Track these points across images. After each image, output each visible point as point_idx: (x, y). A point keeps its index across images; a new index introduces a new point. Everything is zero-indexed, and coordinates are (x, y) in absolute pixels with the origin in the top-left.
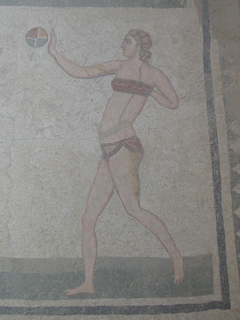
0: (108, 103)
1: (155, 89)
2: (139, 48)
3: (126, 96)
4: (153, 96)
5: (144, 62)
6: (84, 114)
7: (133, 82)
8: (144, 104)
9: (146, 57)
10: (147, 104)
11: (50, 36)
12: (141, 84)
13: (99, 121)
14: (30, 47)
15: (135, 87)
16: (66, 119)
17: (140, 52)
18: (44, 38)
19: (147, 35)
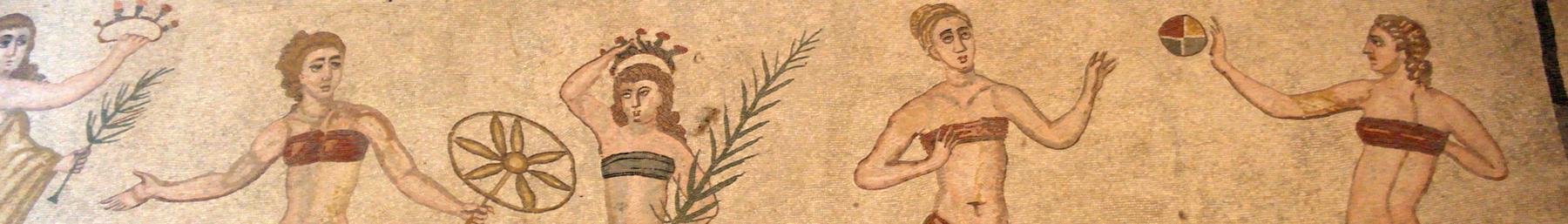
0: (1356, 169)
1: (1452, 138)
2: (1403, 55)
3: (1392, 155)
4: (1449, 155)
5: (1419, 82)
6: (1309, 194)
7: (1404, 126)
8: (1432, 170)
9: (1422, 74)
10: (1439, 171)
11: (1212, 32)
12: (1419, 129)
13: (1343, 207)
14: (1172, 56)
15: (1408, 136)
16: (1272, 204)
17: (1407, 63)
18: (1198, 36)
19: (1416, 26)
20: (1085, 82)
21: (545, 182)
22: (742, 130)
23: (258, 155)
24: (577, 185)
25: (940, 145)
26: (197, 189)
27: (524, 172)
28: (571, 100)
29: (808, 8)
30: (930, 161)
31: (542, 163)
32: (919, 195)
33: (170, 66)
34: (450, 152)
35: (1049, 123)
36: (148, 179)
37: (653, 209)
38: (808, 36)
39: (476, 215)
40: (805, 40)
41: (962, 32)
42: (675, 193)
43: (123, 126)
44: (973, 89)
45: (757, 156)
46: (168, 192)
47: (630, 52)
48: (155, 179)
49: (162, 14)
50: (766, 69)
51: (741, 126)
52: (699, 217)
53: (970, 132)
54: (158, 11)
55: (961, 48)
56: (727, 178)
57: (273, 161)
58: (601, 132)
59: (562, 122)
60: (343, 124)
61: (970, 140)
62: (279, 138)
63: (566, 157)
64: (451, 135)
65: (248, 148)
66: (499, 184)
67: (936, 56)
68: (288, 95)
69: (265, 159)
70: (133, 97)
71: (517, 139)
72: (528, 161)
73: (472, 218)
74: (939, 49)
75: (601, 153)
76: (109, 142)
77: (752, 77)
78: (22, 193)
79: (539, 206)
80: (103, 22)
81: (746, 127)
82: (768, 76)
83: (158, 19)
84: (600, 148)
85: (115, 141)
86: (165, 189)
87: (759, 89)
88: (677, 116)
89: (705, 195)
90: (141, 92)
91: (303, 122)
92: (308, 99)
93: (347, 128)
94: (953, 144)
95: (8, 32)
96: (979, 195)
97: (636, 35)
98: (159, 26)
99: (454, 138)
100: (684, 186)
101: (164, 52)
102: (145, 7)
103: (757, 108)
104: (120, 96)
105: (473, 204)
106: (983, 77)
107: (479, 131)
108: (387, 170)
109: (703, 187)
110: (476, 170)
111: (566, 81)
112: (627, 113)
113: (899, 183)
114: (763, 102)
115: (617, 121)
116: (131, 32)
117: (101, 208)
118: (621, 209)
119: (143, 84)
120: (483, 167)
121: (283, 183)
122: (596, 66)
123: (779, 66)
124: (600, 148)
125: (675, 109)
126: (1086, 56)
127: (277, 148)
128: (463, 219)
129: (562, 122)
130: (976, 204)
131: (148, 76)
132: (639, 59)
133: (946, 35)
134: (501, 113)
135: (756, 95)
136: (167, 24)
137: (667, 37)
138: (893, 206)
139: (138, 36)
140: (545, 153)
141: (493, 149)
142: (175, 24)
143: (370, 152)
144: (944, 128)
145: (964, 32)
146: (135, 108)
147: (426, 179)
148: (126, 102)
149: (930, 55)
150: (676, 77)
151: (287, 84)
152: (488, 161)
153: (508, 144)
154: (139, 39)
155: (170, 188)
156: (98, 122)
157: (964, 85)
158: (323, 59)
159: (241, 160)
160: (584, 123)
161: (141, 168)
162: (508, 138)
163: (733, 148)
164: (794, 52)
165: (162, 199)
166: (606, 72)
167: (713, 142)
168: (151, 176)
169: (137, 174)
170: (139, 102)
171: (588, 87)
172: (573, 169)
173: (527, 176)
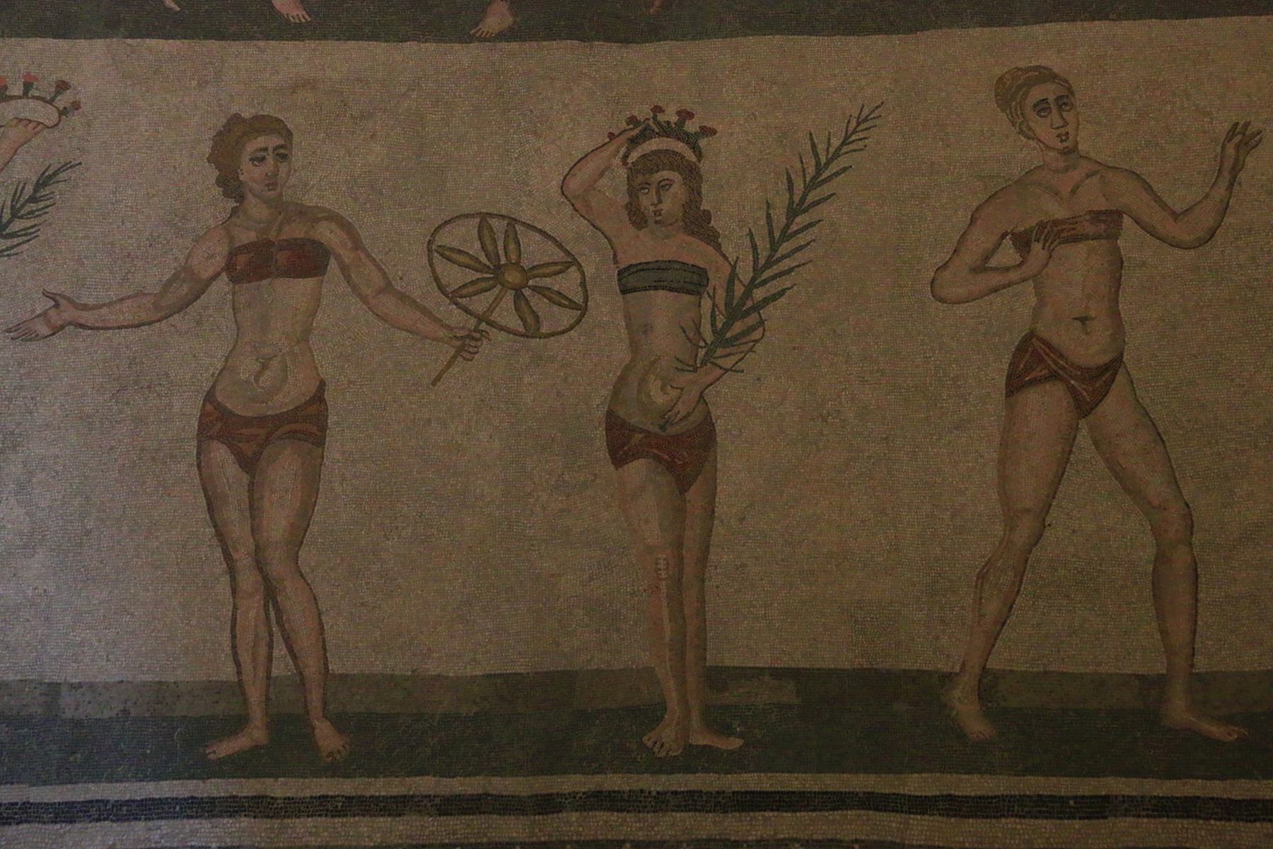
20: (1222, 162)
21: (550, 299)
22: (789, 231)
23: (196, 272)
24: (589, 304)
25: (1036, 247)
26: (126, 313)
27: (524, 288)
28: (574, 197)
29: (865, 75)
30: (1024, 267)
31: (545, 276)
32: (1012, 310)
33: (74, 159)
34: (431, 265)
35: (1175, 215)
36: (62, 301)
37: (684, 332)
38: (866, 111)
39: (467, 341)
40: (863, 117)
41: (1060, 102)
42: (710, 310)
43: (25, 235)
44: (1076, 175)
45: (809, 265)
46: (88, 317)
47: (646, 135)
49: (58, 93)
50: (816, 155)
51: (787, 226)
52: (740, 341)
53: (1074, 229)
54: (53, 89)
55: (1061, 123)
56: (773, 291)
57: (216, 276)
58: (614, 236)
59: (565, 224)
60: (297, 231)
61: (1075, 239)
62: (221, 250)
63: (573, 268)
64: (430, 242)
65: (183, 261)
66: (494, 302)
67: (1031, 134)
68: (227, 194)
69: (205, 275)
70: (33, 199)
71: (512, 246)
72: (528, 273)
73: (464, 345)
74: (1032, 124)
75: (616, 262)
76: (8, 255)
77: (798, 165)
79: (544, 330)
81: (794, 228)
82: (818, 163)
83: (53, 100)
84: (615, 256)
86: (84, 314)
87: (808, 180)
88: (707, 216)
89: (747, 313)
91: (247, 229)
92: (250, 196)
93: (302, 235)
94: (1056, 243)
96: (1087, 308)
97: (652, 115)
98: (57, 109)
99: (434, 247)
100: (721, 302)
101: (66, 141)
103: (806, 205)
104: (15, 199)
105: (463, 328)
106: (1089, 159)
107: (463, 236)
108: (355, 288)
109: (745, 304)
110: (465, 286)
111: (568, 174)
112: (646, 212)
113: (987, 295)
114: (812, 197)
115: (634, 223)
116: (22, 116)
118: (645, 332)
119: (43, 182)
120: (472, 282)
121: (229, 305)
122: (606, 153)
123: (832, 150)
124: (615, 256)
125: (705, 206)
126: (1223, 128)
127: (219, 261)
128: (453, 346)
129: (565, 224)
130: (1083, 320)
131: (50, 172)
132: (654, 145)
133: (1038, 108)
134: (491, 215)
135: (805, 188)
136: (68, 105)
137: (690, 115)
138: (981, 323)
139: (30, 121)
140: (548, 264)
141: (483, 259)
142: (76, 106)
143: (333, 264)
144: (1042, 225)
145: (1064, 101)
146: (37, 213)
147: (403, 297)
149: (1021, 132)
150: (704, 166)
151: (221, 182)
152: (479, 275)
153: (501, 252)
154: (31, 125)
155: (90, 313)
157: (1066, 169)
158: (265, 149)
159: (175, 277)
160: (594, 226)
161: (51, 288)
162: (500, 244)
163: (778, 255)
164: (849, 134)
166: (617, 161)
167: (754, 247)
168: (64, 297)
169: (46, 294)
170: (41, 205)
171: (595, 181)
172: (583, 284)
173: (527, 292)
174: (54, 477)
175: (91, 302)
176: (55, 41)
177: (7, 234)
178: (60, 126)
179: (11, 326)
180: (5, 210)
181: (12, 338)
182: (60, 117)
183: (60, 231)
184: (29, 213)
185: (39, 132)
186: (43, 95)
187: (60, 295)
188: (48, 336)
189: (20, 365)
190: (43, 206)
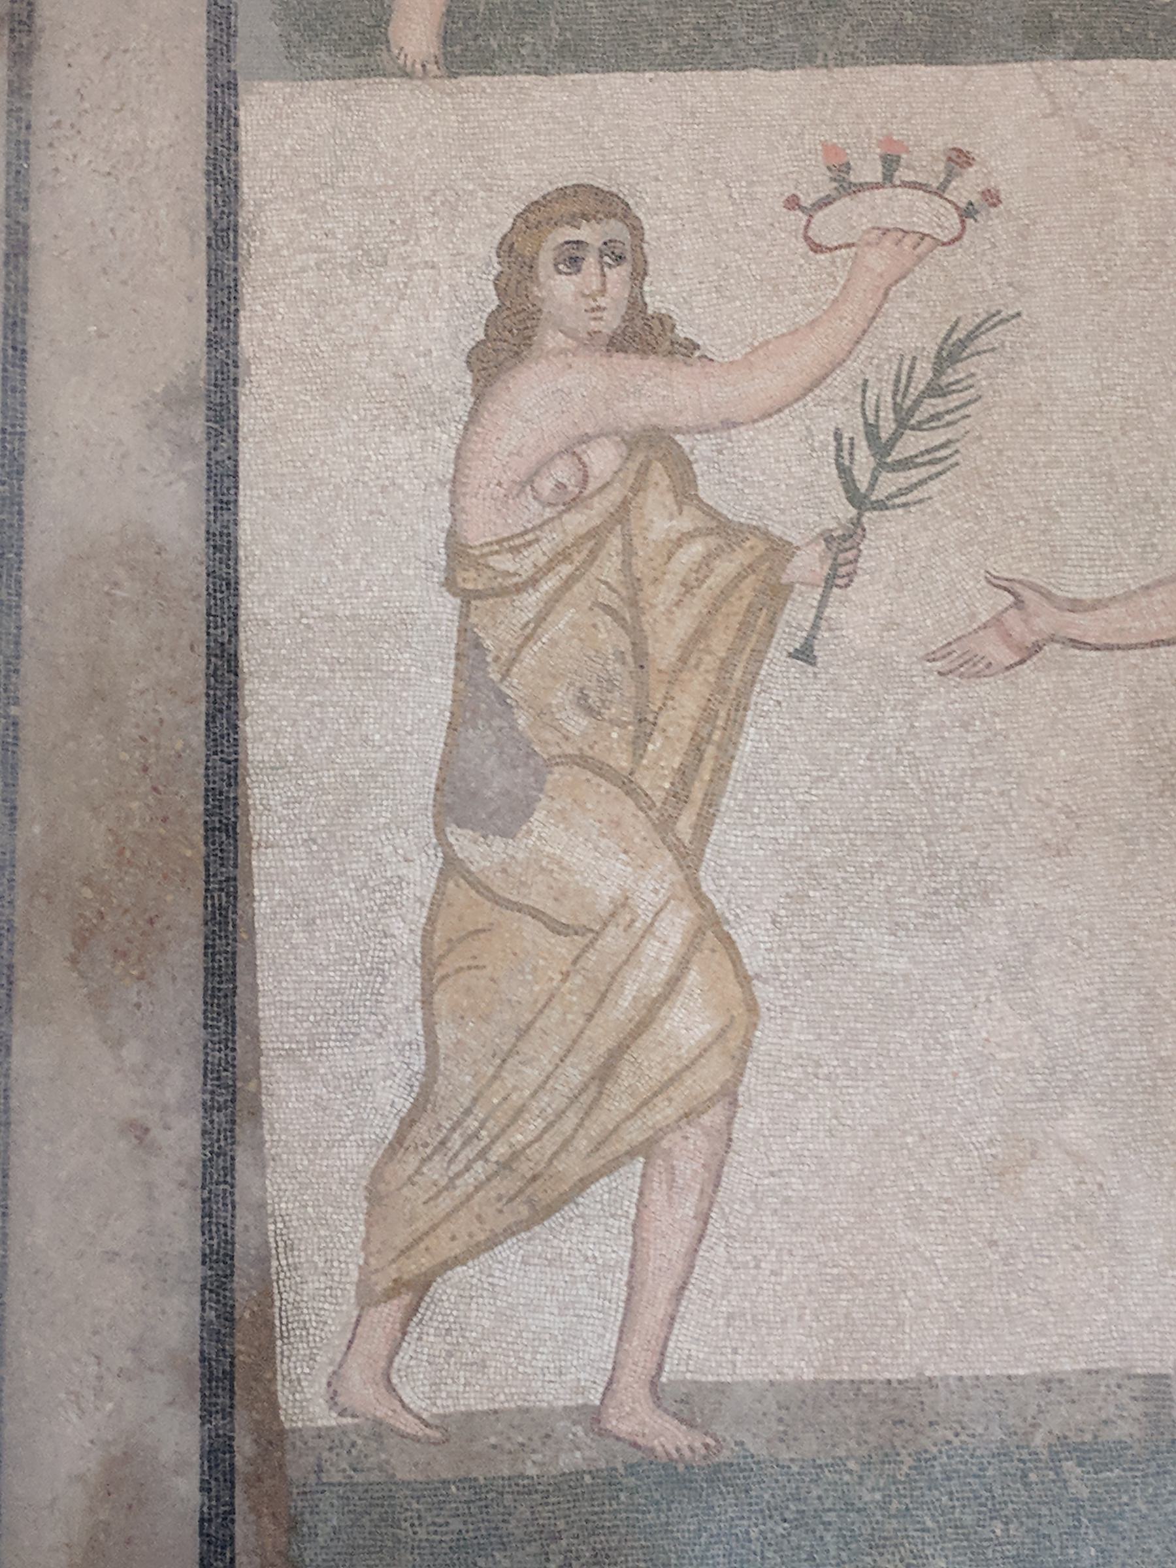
33: (1005, 305)
36: (1027, 594)
43: (931, 462)
46: (1086, 626)
48: (1048, 596)
49: (950, 175)
54: (940, 167)
70: (935, 390)
76: (905, 505)
78: (720, 642)
80: (806, 202)
83: (944, 186)
85: (921, 501)
86: (1070, 616)
90: (950, 377)
95: (572, 234)
98: (957, 208)
101: (983, 270)
102: (904, 156)
104: (899, 387)
116: (887, 222)
117: (930, 671)
136: (975, 198)
146: (948, 418)
148: (917, 402)
154: (908, 241)
155: (1089, 616)
156: (863, 456)
165: (1076, 643)
169: (996, 583)
170: (954, 400)
174: (1074, 953)
175: (1087, 593)
176: (929, 69)
177: (899, 462)
178: (966, 240)
179: (934, 648)
180: (882, 414)
181: (940, 673)
182: (963, 222)
183: (1000, 452)
184: (933, 418)
185: (926, 254)
186: (922, 179)
187: (1020, 582)
188: (1012, 666)
189: (965, 726)
190: (957, 403)
